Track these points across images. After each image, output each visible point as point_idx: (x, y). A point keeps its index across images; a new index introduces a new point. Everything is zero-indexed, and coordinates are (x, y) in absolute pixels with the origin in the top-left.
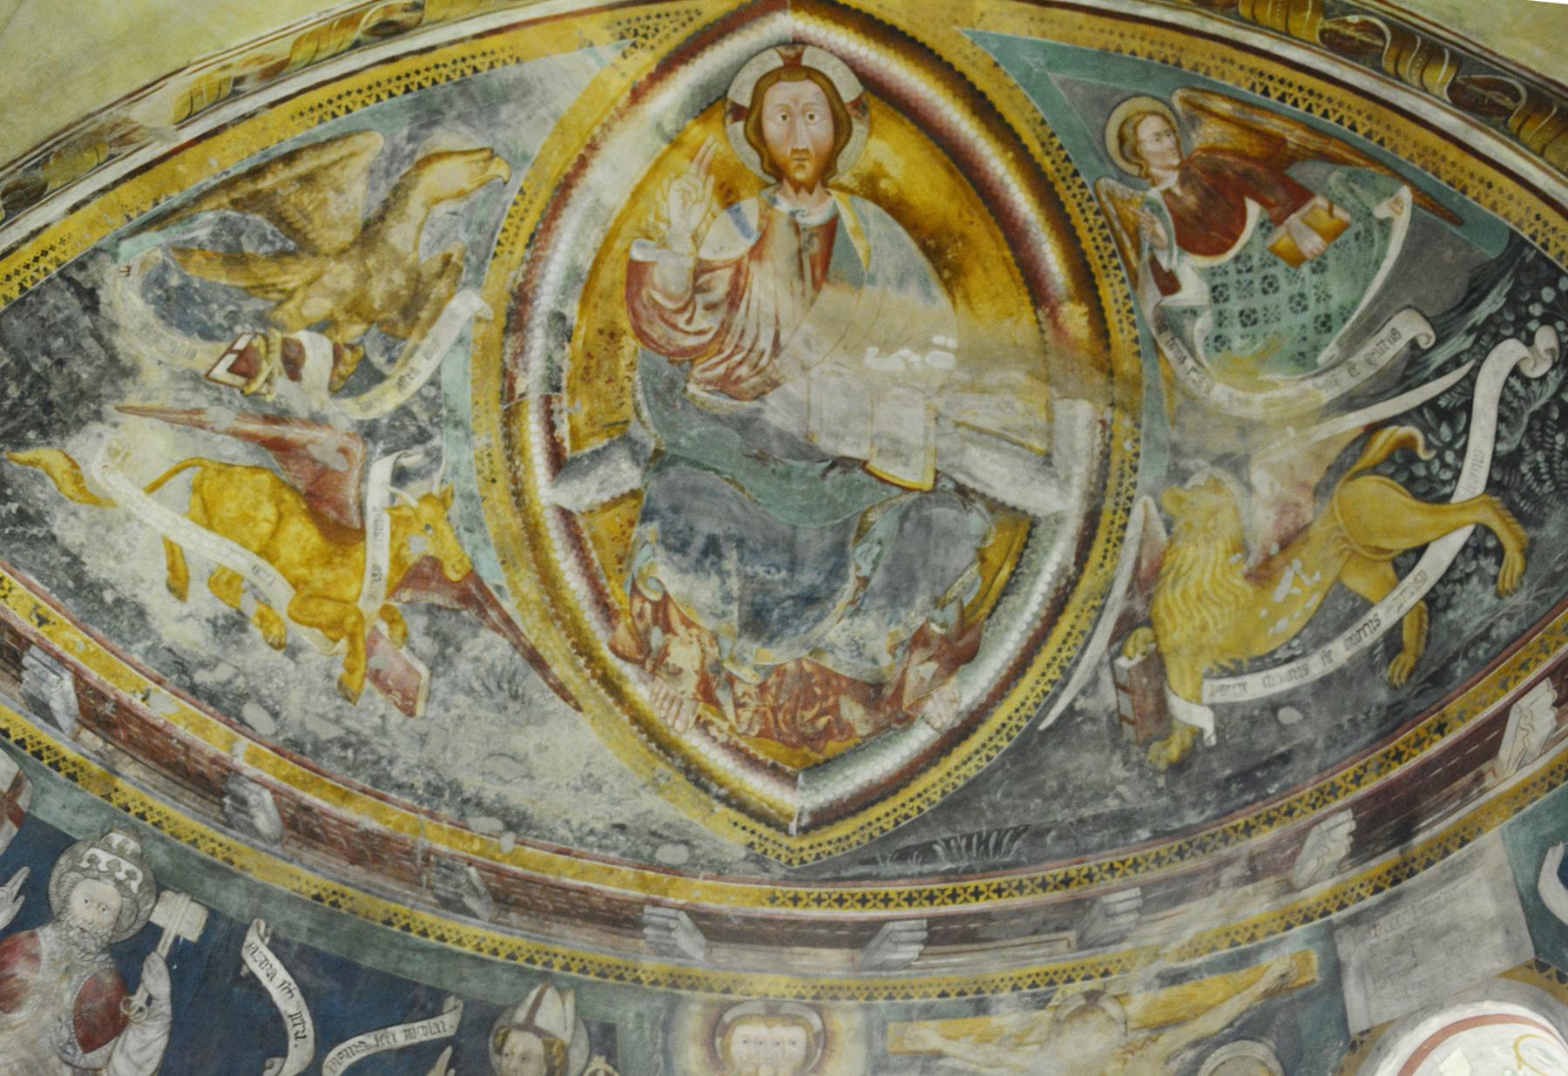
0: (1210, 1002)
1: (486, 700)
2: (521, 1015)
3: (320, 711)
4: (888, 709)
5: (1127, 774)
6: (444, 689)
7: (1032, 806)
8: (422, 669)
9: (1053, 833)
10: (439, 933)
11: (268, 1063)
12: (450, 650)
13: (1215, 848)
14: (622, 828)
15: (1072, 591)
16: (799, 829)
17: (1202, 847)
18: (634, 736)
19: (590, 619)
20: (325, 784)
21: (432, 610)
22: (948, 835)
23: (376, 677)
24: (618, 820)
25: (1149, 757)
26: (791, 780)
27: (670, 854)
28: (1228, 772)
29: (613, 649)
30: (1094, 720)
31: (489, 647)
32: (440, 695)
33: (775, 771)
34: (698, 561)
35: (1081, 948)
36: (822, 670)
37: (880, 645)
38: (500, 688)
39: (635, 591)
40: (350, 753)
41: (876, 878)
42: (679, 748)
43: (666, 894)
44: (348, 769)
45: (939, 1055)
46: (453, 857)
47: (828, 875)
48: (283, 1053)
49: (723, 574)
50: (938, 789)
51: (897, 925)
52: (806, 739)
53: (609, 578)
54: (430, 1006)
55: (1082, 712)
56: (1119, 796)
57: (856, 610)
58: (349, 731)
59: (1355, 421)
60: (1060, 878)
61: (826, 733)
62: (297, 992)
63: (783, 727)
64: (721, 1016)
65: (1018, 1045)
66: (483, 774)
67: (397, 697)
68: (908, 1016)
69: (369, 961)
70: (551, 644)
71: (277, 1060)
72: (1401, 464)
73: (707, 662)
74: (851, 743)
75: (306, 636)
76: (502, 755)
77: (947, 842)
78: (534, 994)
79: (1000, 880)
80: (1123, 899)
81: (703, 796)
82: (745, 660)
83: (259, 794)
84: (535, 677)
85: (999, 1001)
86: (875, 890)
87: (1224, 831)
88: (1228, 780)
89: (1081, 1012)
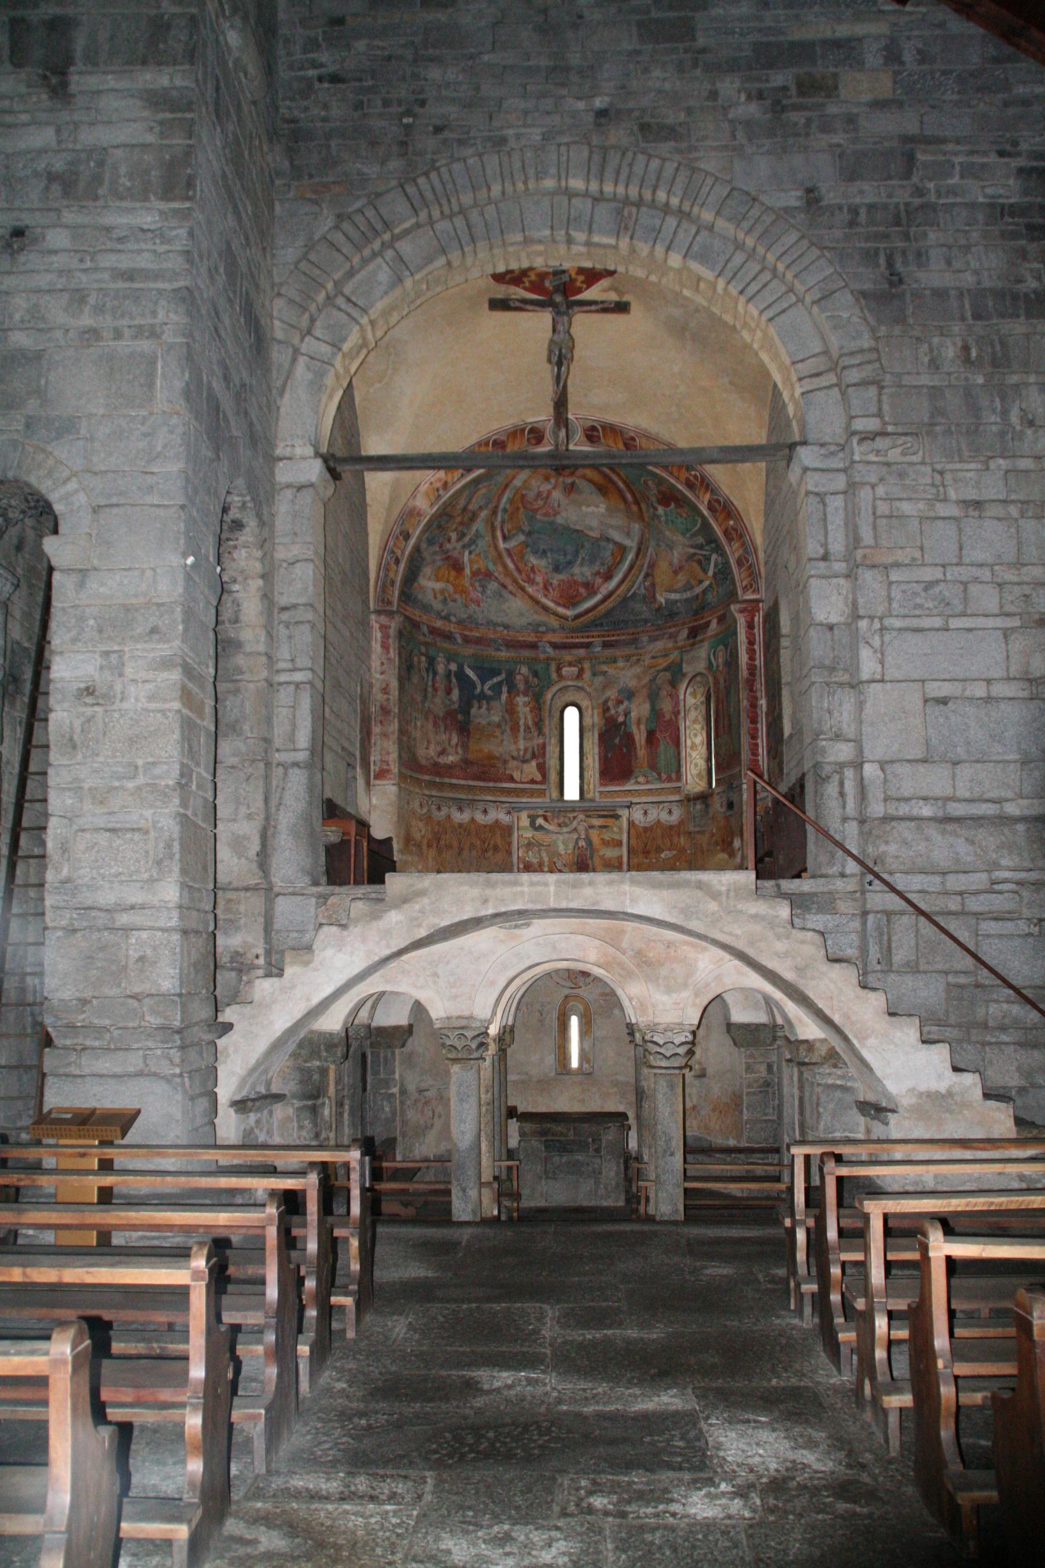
19: (516, 574)
27: (542, 629)
33: (565, 606)
37: (588, 574)
57: (582, 565)
59: (692, 551)
69: (486, 665)
72: (699, 562)
75: (457, 596)
80: (645, 639)
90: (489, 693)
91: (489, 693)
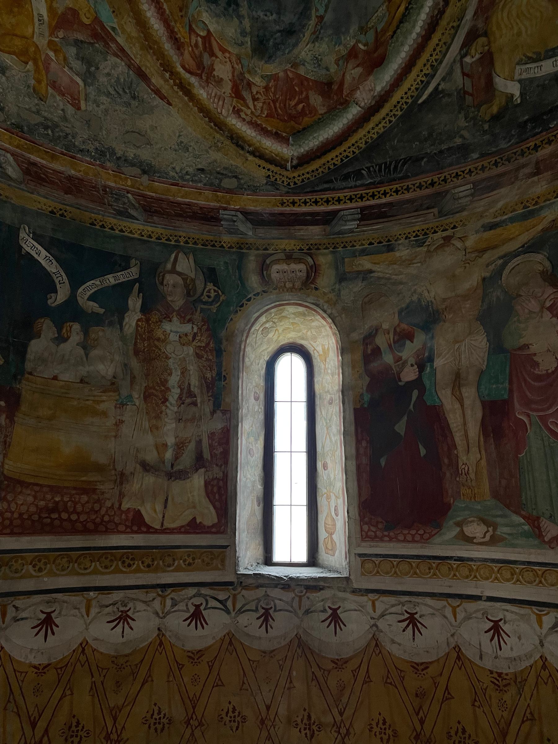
0: (511, 236)
1: (119, 100)
2: (169, 266)
3: (27, 107)
4: (335, 97)
5: (467, 124)
6: (93, 93)
7: (414, 146)
8: (79, 80)
9: (425, 160)
10: (120, 228)
11: (48, 296)
12: (93, 68)
13: (516, 159)
14: (202, 170)
15: (441, 17)
16: (292, 167)
17: (509, 160)
18: (202, 120)
20: (40, 149)
21: (77, 43)
22: (369, 165)
23: (54, 85)
24: (200, 166)
25: (480, 114)
26: (285, 140)
28: (527, 117)
29: (184, 67)
30: (449, 95)
31: (114, 67)
32: (92, 97)
33: (277, 136)
34: (225, 9)
35: (440, 217)
36: (299, 76)
37: (330, 60)
38: (125, 92)
39: (191, 30)
40: (50, 132)
41: (334, 189)
42: (226, 125)
43: (229, 204)
44: (51, 141)
45: (371, 271)
46: (119, 189)
47: (308, 190)
48: (56, 292)
49: (240, 17)
50: (363, 141)
51: (346, 212)
52: (292, 117)
53: (176, 21)
54: (123, 264)
55: (443, 91)
56: (462, 136)
57: (316, 38)
58: (46, 119)
60: (430, 182)
61: (303, 113)
62: (54, 261)
63: (279, 110)
64: (265, 261)
65: (410, 264)
66: (125, 143)
67: (69, 98)
68: (354, 255)
69: (88, 243)
70: (149, 65)
71: (52, 295)
73: (236, 74)
74: (316, 118)
76: (132, 132)
77: (368, 168)
78: (173, 256)
79: (397, 186)
81: (241, 152)
82: (256, 71)
83: (4, 156)
84: (143, 84)
85: (399, 244)
86: (333, 196)
87: (522, 150)
88: (526, 122)
89: (441, 246)
90: (93, 307)
91: (93, 307)
